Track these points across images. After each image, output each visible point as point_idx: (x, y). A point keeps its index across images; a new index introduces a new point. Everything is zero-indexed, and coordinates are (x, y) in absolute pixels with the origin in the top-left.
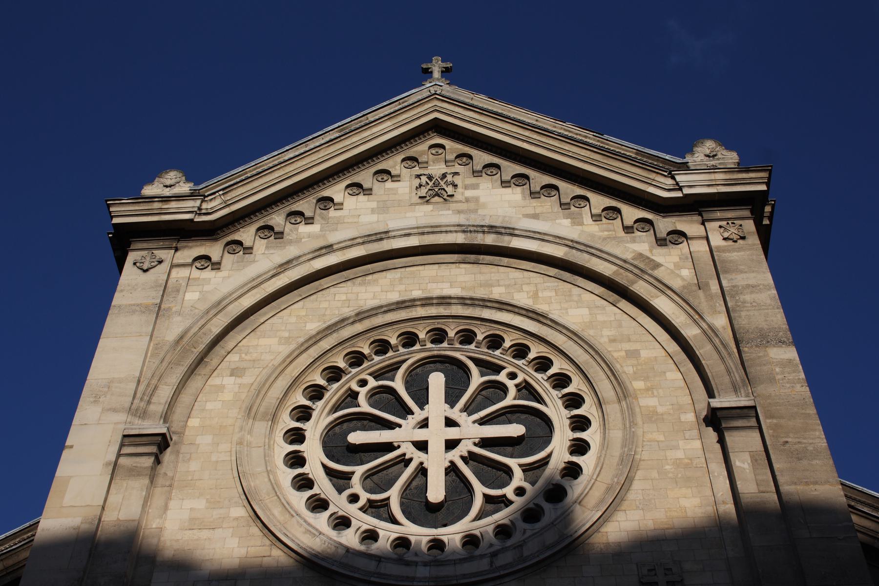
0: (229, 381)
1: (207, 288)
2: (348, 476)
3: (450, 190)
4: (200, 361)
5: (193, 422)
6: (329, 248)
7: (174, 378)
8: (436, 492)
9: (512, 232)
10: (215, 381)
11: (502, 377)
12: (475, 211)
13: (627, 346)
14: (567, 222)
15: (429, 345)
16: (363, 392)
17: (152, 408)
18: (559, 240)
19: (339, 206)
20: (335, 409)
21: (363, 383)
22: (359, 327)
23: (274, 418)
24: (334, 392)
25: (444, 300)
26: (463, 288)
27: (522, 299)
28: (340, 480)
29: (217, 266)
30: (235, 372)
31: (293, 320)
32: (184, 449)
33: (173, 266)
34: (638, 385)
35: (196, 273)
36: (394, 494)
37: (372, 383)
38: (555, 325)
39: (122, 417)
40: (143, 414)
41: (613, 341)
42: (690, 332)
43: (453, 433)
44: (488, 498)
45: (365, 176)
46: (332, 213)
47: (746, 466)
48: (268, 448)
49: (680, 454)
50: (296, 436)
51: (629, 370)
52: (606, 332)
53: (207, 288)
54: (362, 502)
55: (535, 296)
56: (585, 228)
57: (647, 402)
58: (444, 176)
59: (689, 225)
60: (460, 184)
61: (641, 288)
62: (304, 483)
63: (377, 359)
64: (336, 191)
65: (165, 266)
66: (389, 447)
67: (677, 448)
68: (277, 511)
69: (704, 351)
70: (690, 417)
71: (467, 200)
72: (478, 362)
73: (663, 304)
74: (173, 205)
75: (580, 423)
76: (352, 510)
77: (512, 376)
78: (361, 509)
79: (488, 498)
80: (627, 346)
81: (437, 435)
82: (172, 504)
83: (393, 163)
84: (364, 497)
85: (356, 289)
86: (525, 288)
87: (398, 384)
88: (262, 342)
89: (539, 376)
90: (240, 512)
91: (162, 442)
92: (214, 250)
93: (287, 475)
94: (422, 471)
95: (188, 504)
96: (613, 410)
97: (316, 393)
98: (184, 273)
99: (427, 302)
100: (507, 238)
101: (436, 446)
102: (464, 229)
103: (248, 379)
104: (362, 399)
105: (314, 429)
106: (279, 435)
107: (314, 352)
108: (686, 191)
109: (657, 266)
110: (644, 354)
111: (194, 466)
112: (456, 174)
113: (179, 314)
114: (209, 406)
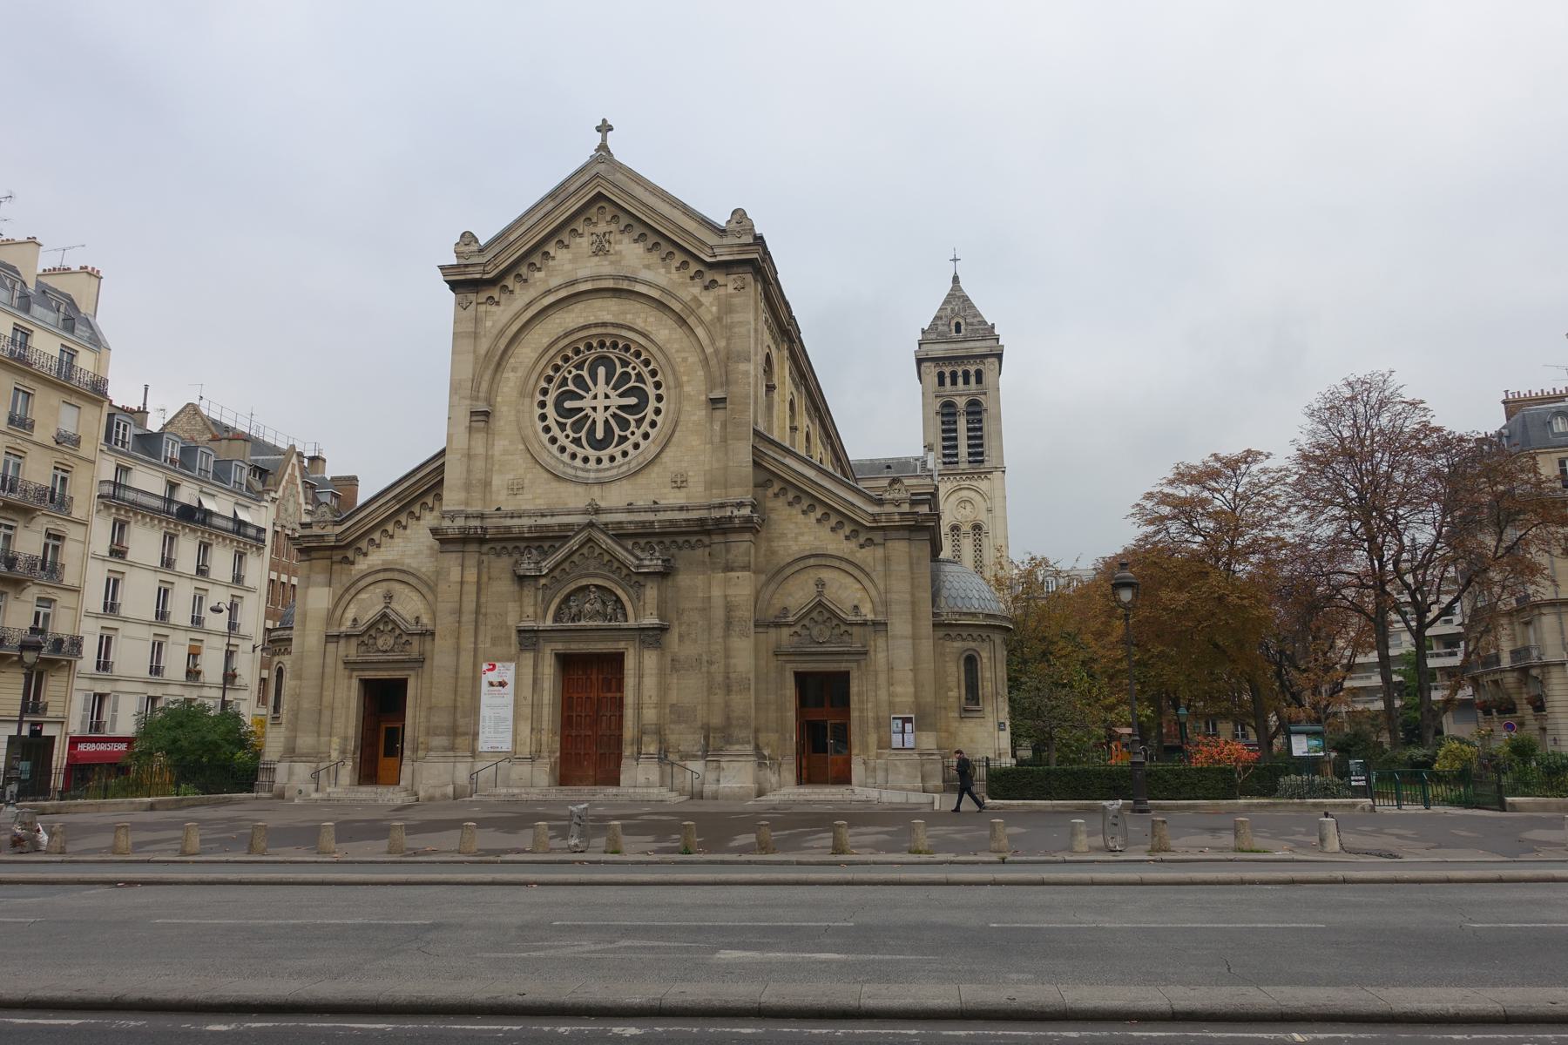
0: (511, 375)
1: (495, 318)
2: (565, 424)
3: (607, 245)
4: (499, 364)
5: (499, 399)
6: (549, 292)
7: (487, 377)
8: (600, 434)
9: (635, 280)
10: (505, 375)
11: (629, 369)
12: (620, 261)
13: (683, 355)
14: (663, 271)
15: (599, 350)
16: (570, 377)
17: (480, 394)
18: (657, 287)
19: (553, 258)
20: (559, 387)
21: (570, 372)
22: (566, 341)
23: (532, 396)
24: (558, 378)
25: (604, 325)
26: (614, 315)
27: (639, 324)
28: (562, 427)
29: (498, 303)
30: (514, 370)
31: (536, 336)
32: (497, 414)
33: (478, 304)
34: (685, 378)
35: (489, 308)
36: (583, 434)
37: (574, 372)
38: (652, 341)
39: (468, 402)
40: (477, 399)
41: (677, 351)
42: (709, 350)
43: (607, 402)
44: (619, 436)
45: (565, 236)
46: (551, 263)
47: (718, 428)
48: (532, 412)
49: (695, 418)
50: (543, 405)
51: (682, 370)
52: (676, 346)
53: (495, 318)
54: (570, 439)
55: (645, 321)
56: (672, 276)
57: (687, 389)
58: (605, 234)
59: (721, 279)
60: (612, 240)
61: (691, 321)
62: (547, 429)
63: (576, 358)
64: (551, 248)
65: (474, 303)
66: (581, 410)
67: (695, 414)
68: (536, 446)
69: (713, 362)
70: (703, 398)
71: (616, 253)
72: (619, 359)
73: (700, 332)
74: (470, 269)
75: (659, 398)
76: (566, 443)
77: (634, 368)
78: (571, 442)
79: (619, 436)
80: (683, 355)
81: (600, 403)
82: (496, 442)
83: (579, 225)
84: (572, 435)
85: (565, 315)
86: (642, 315)
87: (585, 373)
88: (524, 350)
89: (645, 369)
90: (521, 447)
91: (487, 414)
92: (495, 293)
93: (540, 425)
94: (594, 422)
95: (502, 442)
96: (672, 392)
97: (549, 380)
98: (482, 308)
99: (596, 325)
100: (633, 283)
101: (600, 409)
102: (614, 278)
103: (519, 374)
104: (569, 382)
105: (550, 399)
106: (536, 404)
107: (547, 357)
108: (719, 258)
109: (700, 304)
110: (690, 360)
111: (502, 423)
112: (611, 232)
113: (485, 336)
114: (505, 389)
